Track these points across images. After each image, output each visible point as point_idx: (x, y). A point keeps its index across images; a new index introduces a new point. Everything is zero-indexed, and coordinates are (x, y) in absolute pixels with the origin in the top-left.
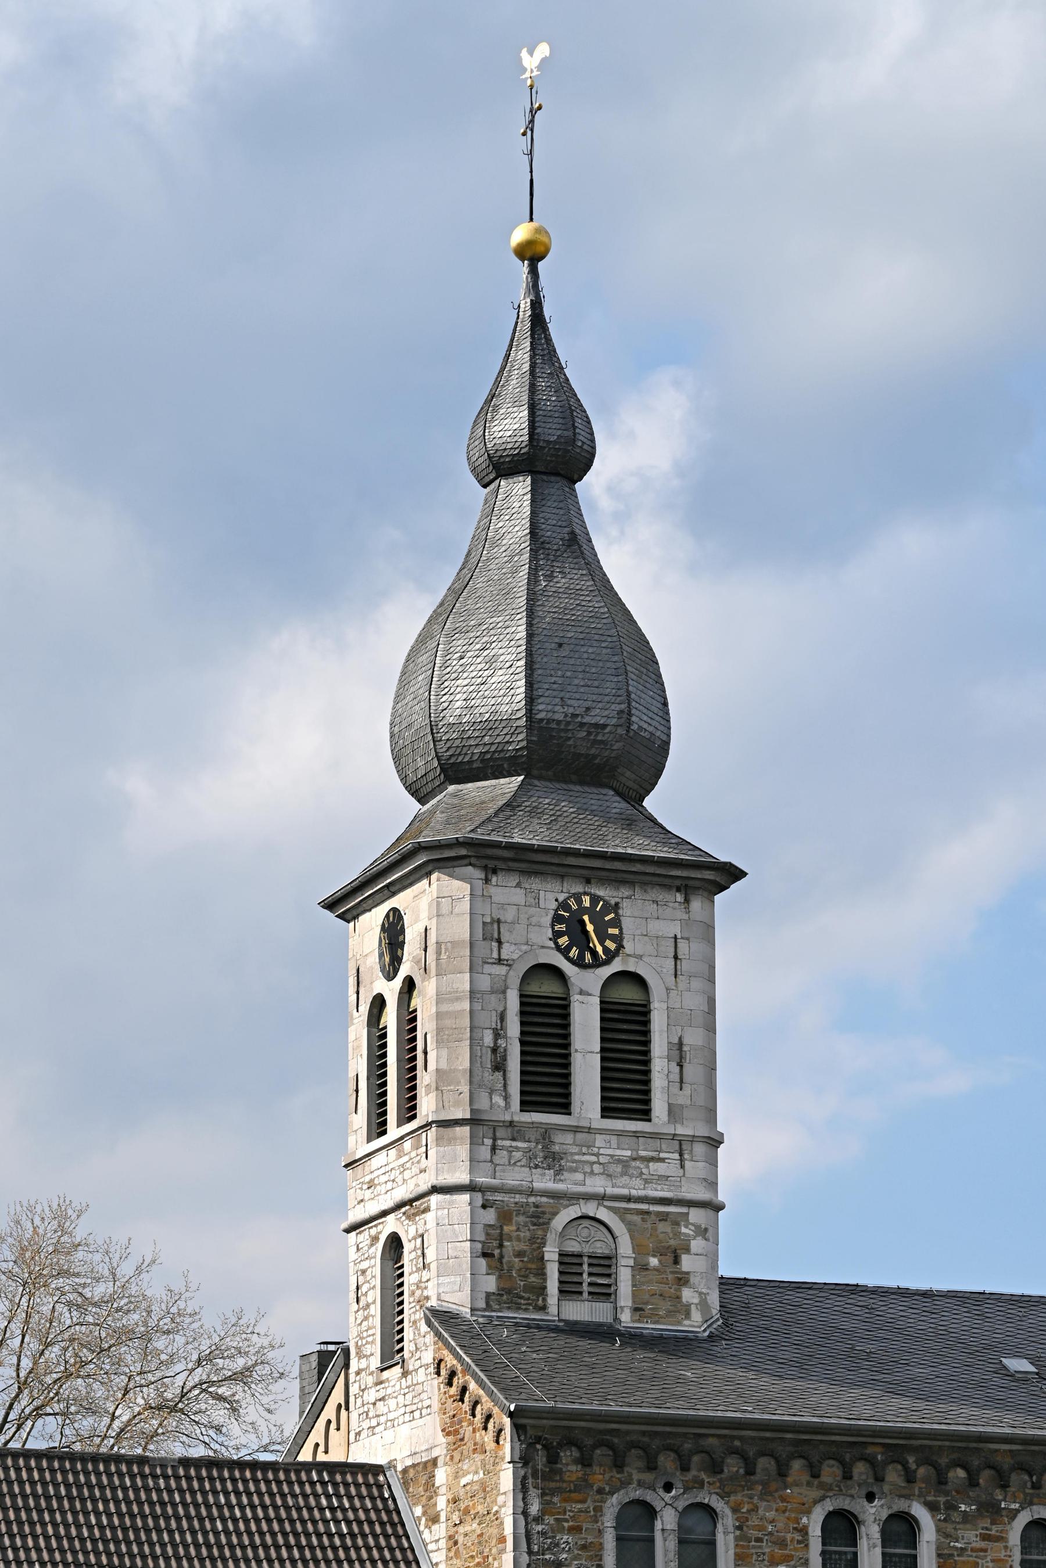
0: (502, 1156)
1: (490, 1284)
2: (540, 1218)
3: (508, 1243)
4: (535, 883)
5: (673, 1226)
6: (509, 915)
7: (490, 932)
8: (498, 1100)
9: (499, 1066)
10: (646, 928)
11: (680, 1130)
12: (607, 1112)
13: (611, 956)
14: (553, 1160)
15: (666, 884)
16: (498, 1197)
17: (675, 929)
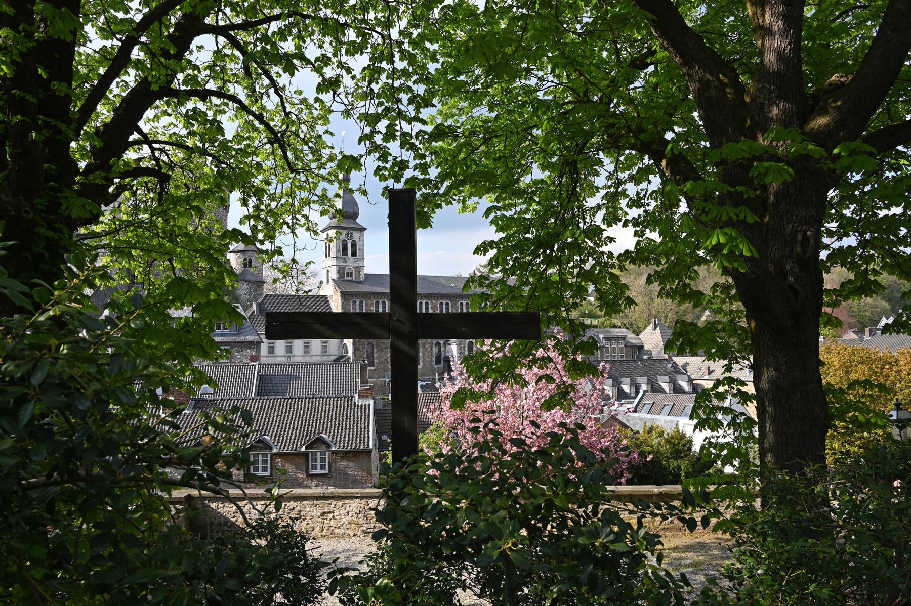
2: (344, 268)
3: (341, 271)
5: (359, 269)
10: (356, 235)
14: (345, 262)
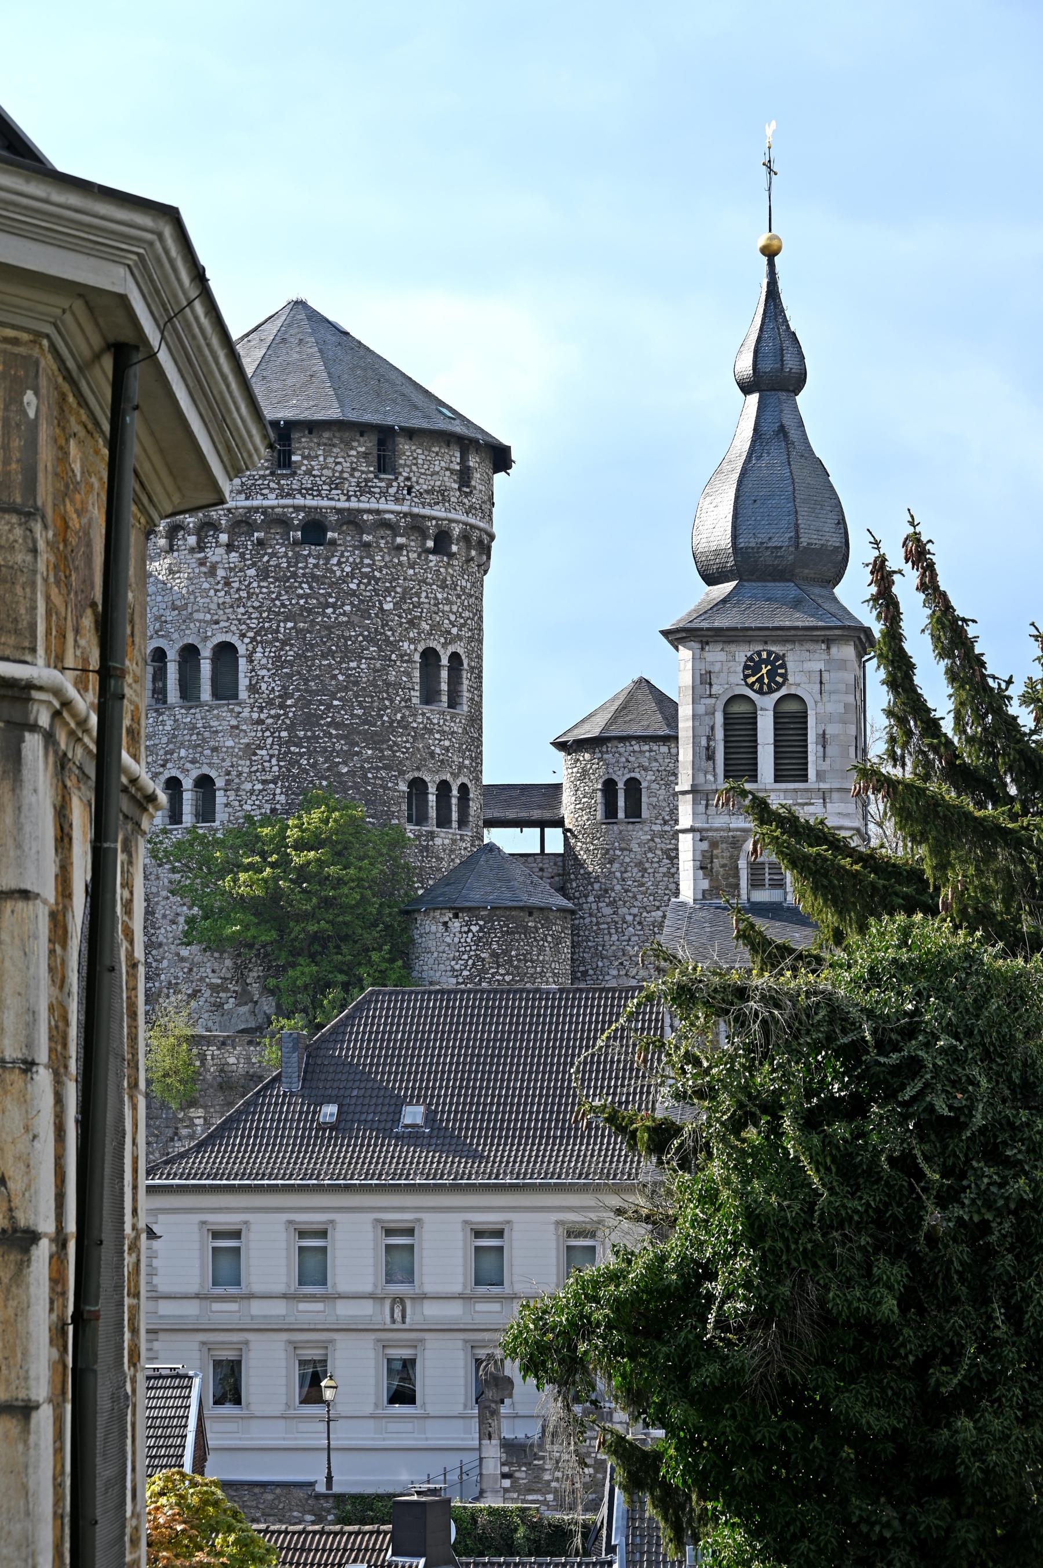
0: (712, 810)
1: (705, 884)
4: (732, 648)
6: (717, 668)
7: (704, 680)
8: (710, 777)
9: (711, 757)
11: (822, 786)
12: (778, 778)
13: (779, 686)
15: (815, 640)
16: (710, 834)
17: (821, 666)
